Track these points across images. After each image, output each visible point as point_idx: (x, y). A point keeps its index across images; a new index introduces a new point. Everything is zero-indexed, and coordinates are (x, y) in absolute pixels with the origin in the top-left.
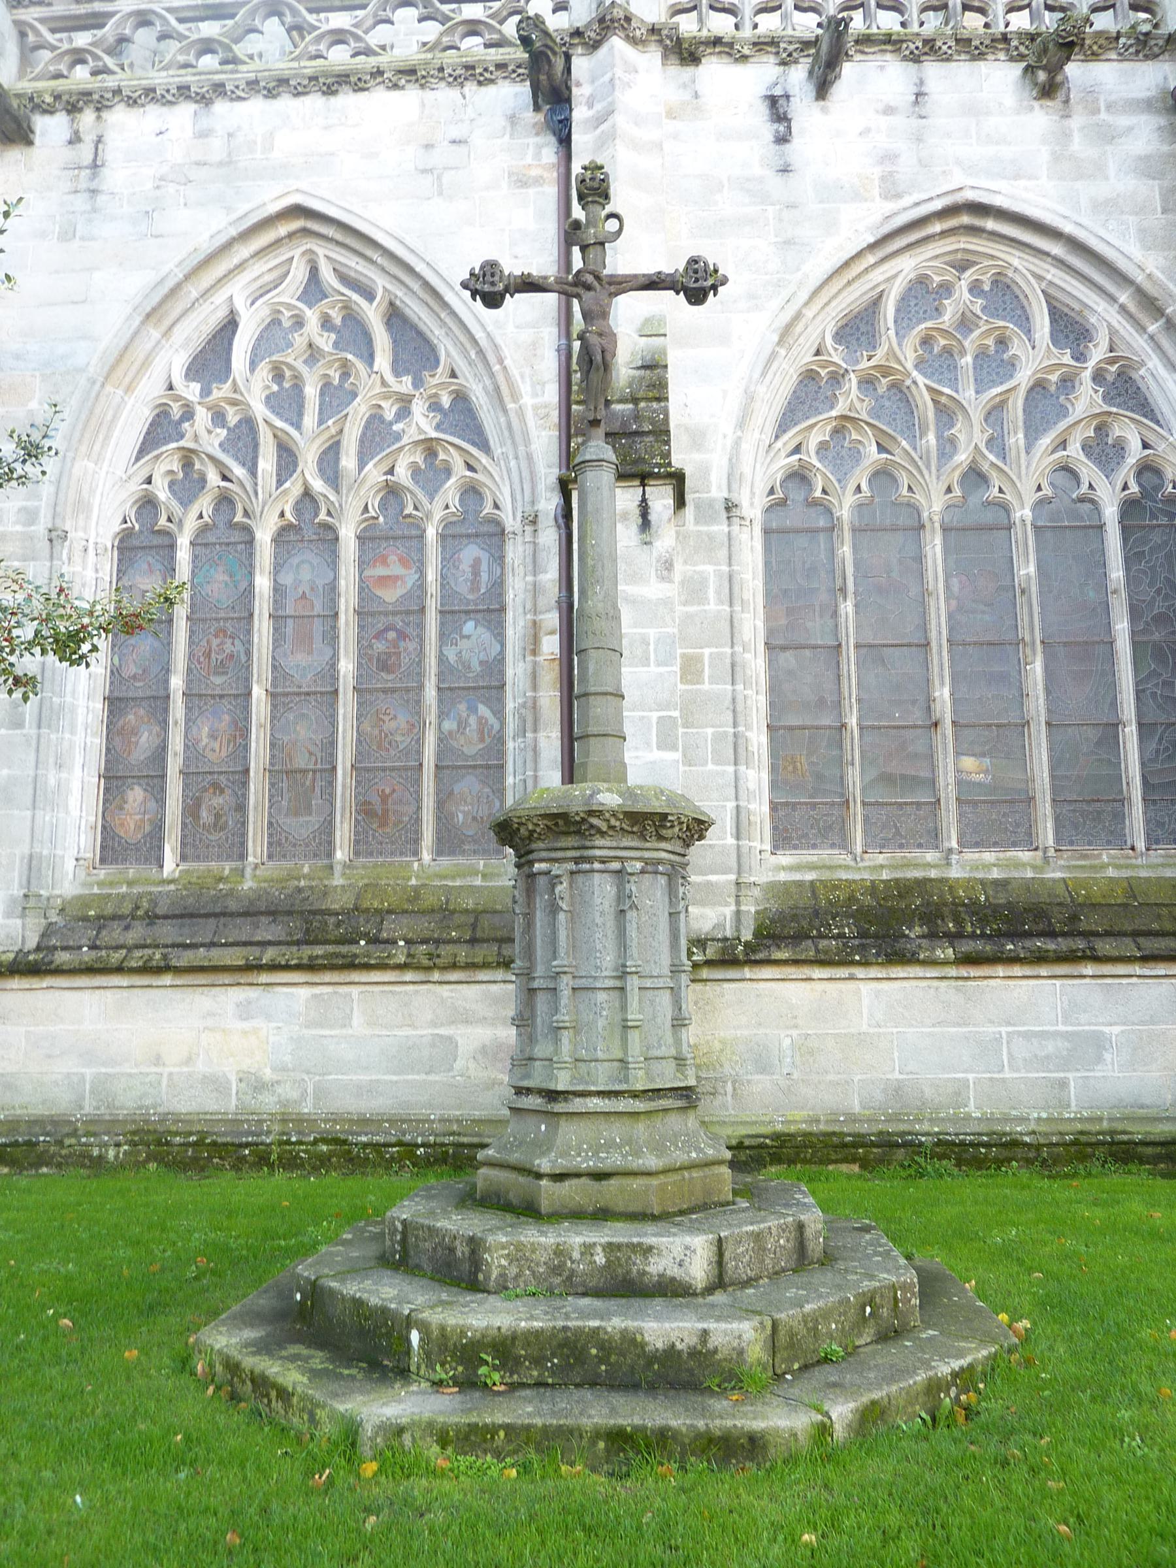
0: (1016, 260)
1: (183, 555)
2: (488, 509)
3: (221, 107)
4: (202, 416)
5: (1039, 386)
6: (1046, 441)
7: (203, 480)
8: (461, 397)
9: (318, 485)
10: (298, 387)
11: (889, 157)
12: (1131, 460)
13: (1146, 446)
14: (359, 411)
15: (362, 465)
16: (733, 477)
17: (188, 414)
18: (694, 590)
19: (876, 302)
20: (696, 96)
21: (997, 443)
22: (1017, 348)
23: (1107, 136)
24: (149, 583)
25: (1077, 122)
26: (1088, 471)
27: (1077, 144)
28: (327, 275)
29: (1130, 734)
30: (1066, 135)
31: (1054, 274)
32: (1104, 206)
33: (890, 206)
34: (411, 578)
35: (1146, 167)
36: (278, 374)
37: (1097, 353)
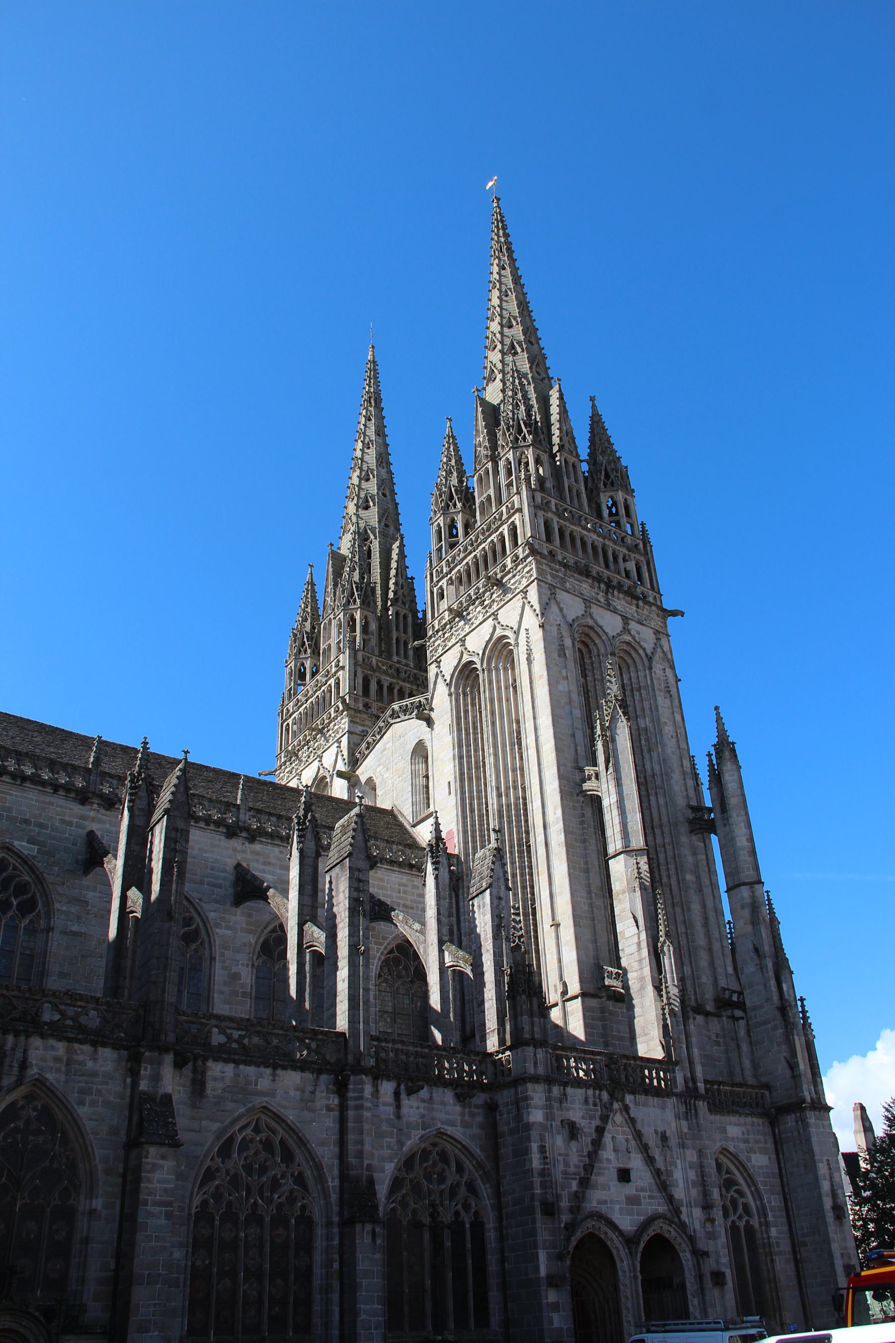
0: (449, 1146)
3: (242, 1067)
8: (301, 1174)
11: (423, 1116)
12: (473, 1210)
13: (476, 1206)
22: (447, 1173)
25: (466, 1111)
26: (463, 1213)
31: (457, 1151)
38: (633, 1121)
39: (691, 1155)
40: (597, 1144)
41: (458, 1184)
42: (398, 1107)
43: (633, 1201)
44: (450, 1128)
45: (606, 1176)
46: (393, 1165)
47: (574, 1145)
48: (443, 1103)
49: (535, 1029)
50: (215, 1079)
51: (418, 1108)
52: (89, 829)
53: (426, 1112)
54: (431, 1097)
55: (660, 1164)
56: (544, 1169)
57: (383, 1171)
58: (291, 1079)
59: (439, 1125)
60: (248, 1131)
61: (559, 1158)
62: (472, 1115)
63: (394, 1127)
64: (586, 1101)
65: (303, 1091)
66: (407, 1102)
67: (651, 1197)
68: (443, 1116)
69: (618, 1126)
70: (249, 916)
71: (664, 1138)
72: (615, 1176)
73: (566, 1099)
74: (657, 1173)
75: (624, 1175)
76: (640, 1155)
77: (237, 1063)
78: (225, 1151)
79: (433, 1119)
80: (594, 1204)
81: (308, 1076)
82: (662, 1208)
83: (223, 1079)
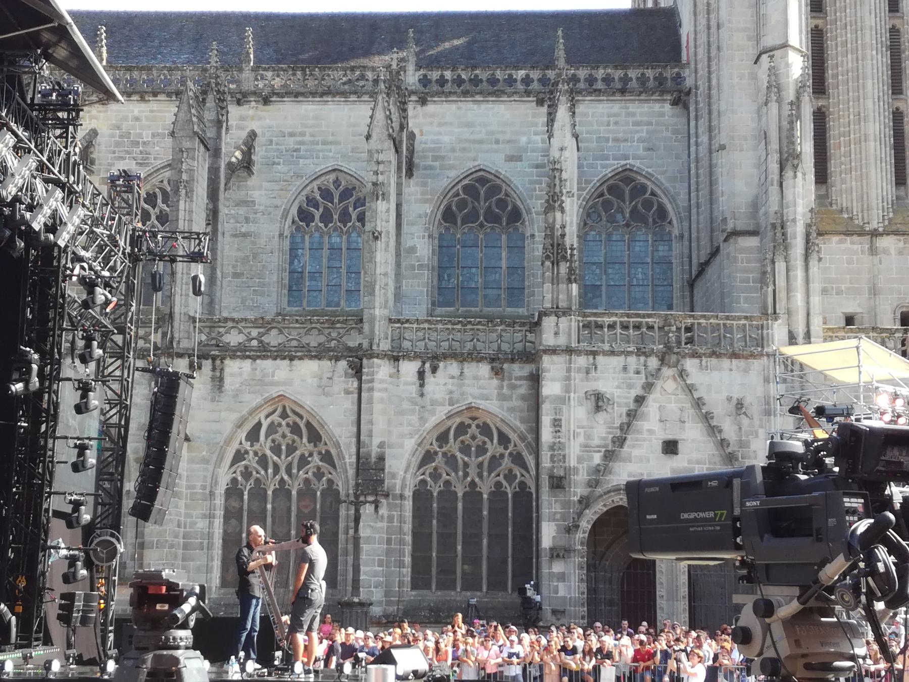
1: (246, 497)
2: (335, 487)
3: (258, 361)
4: (251, 453)
5: (493, 458)
6: (493, 475)
7: (251, 473)
9: (286, 477)
10: (279, 446)
11: (451, 392)
14: (298, 453)
15: (299, 471)
16: (403, 486)
17: (247, 452)
18: (390, 519)
19: (449, 429)
20: (398, 371)
21: (480, 476)
22: (489, 445)
23: (513, 387)
24: (236, 504)
25: (505, 383)
26: (505, 483)
27: (505, 391)
28: (289, 412)
29: (510, 560)
30: (501, 387)
32: (511, 410)
33: (451, 408)
34: (312, 506)
35: (523, 398)
36: (273, 441)
37: (511, 448)
38: (690, 389)
41: (502, 456)
42: (422, 385)
44: (483, 402)
46: (413, 441)
47: (602, 417)
48: (476, 378)
49: (561, 296)
50: (232, 375)
51: (445, 384)
52: (248, 130)
53: (454, 388)
54: (462, 373)
56: (555, 443)
57: (402, 446)
58: (308, 368)
59: (470, 400)
60: (275, 417)
61: (579, 430)
62: (513, 387)
63: (416, 404)
65: (321, 379)
66: (432, 379)
68: (476, 391)
69: (669, 394)
70: (425, 184)
72: (659, 448)
73: (596, 368)
76: (700, 425)
77: (254, 358)
78: (253, 436)
79: (462, 394)
81: (326, 364)
83: (241, 374)
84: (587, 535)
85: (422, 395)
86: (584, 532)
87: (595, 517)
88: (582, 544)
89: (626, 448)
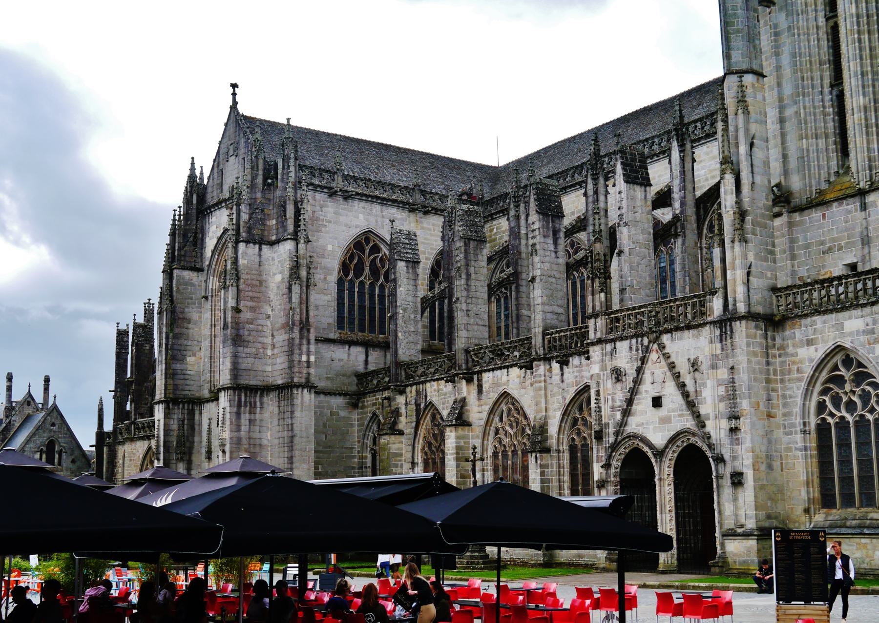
38: (667, 356)
39: (723, 373)
40: (637, 381)
42: (562, 375)
43: (665, 420)
45: (643, 404)
47: (619, 385)
51: (573, 372)
55: (690, 388)
64: (631, 348)
67: (680, 416)
71: (695, 366)
74: (686, 395)
75: (657, 402)
80: (634, 426)
82: (689, 423)
84: (618, 470)
85: (563, 381)
86: (616, 468)
87: (623, 457)
88: (615, 476)
89: (634, 407)
